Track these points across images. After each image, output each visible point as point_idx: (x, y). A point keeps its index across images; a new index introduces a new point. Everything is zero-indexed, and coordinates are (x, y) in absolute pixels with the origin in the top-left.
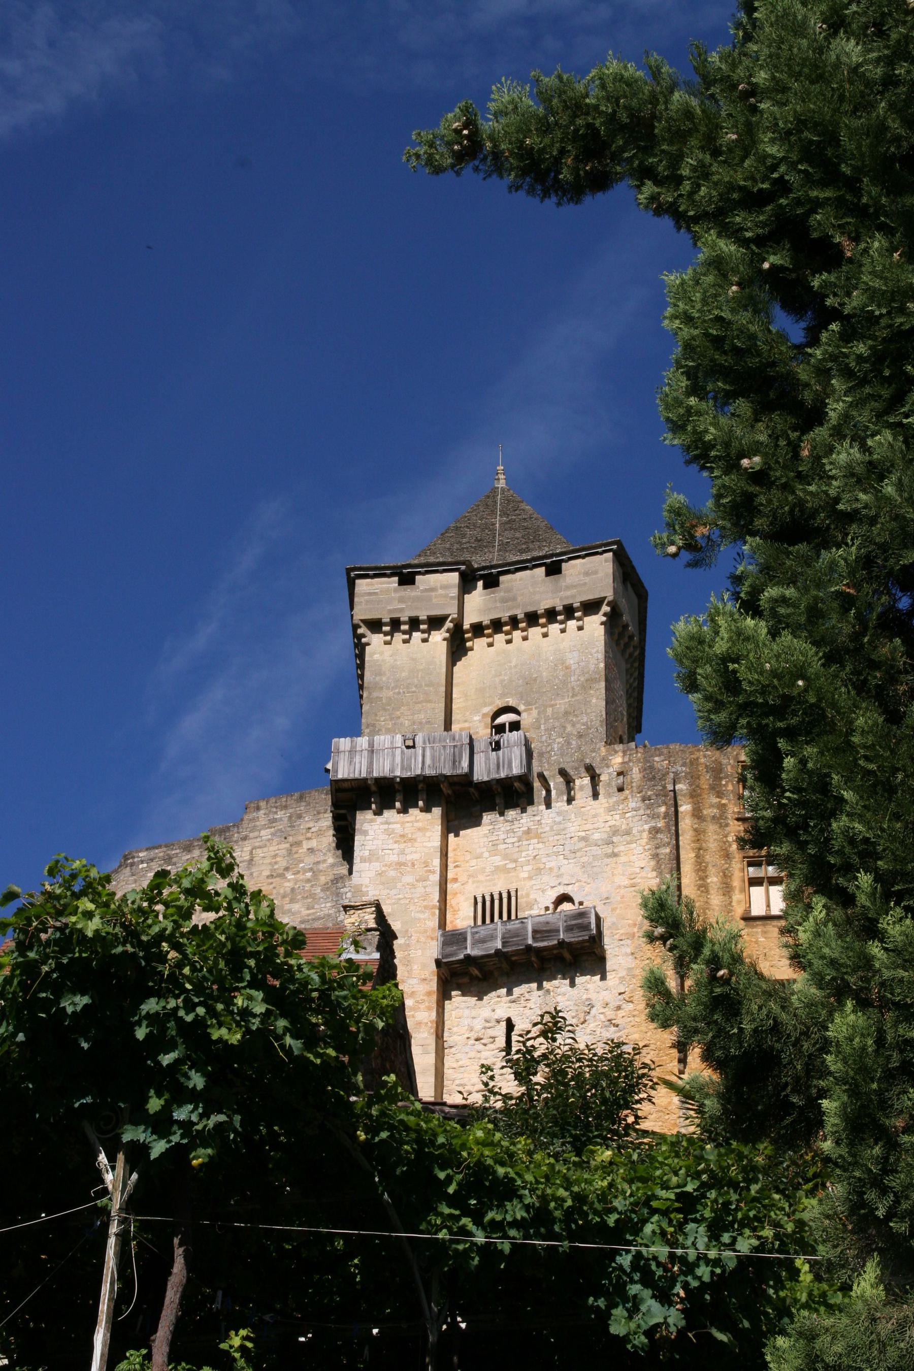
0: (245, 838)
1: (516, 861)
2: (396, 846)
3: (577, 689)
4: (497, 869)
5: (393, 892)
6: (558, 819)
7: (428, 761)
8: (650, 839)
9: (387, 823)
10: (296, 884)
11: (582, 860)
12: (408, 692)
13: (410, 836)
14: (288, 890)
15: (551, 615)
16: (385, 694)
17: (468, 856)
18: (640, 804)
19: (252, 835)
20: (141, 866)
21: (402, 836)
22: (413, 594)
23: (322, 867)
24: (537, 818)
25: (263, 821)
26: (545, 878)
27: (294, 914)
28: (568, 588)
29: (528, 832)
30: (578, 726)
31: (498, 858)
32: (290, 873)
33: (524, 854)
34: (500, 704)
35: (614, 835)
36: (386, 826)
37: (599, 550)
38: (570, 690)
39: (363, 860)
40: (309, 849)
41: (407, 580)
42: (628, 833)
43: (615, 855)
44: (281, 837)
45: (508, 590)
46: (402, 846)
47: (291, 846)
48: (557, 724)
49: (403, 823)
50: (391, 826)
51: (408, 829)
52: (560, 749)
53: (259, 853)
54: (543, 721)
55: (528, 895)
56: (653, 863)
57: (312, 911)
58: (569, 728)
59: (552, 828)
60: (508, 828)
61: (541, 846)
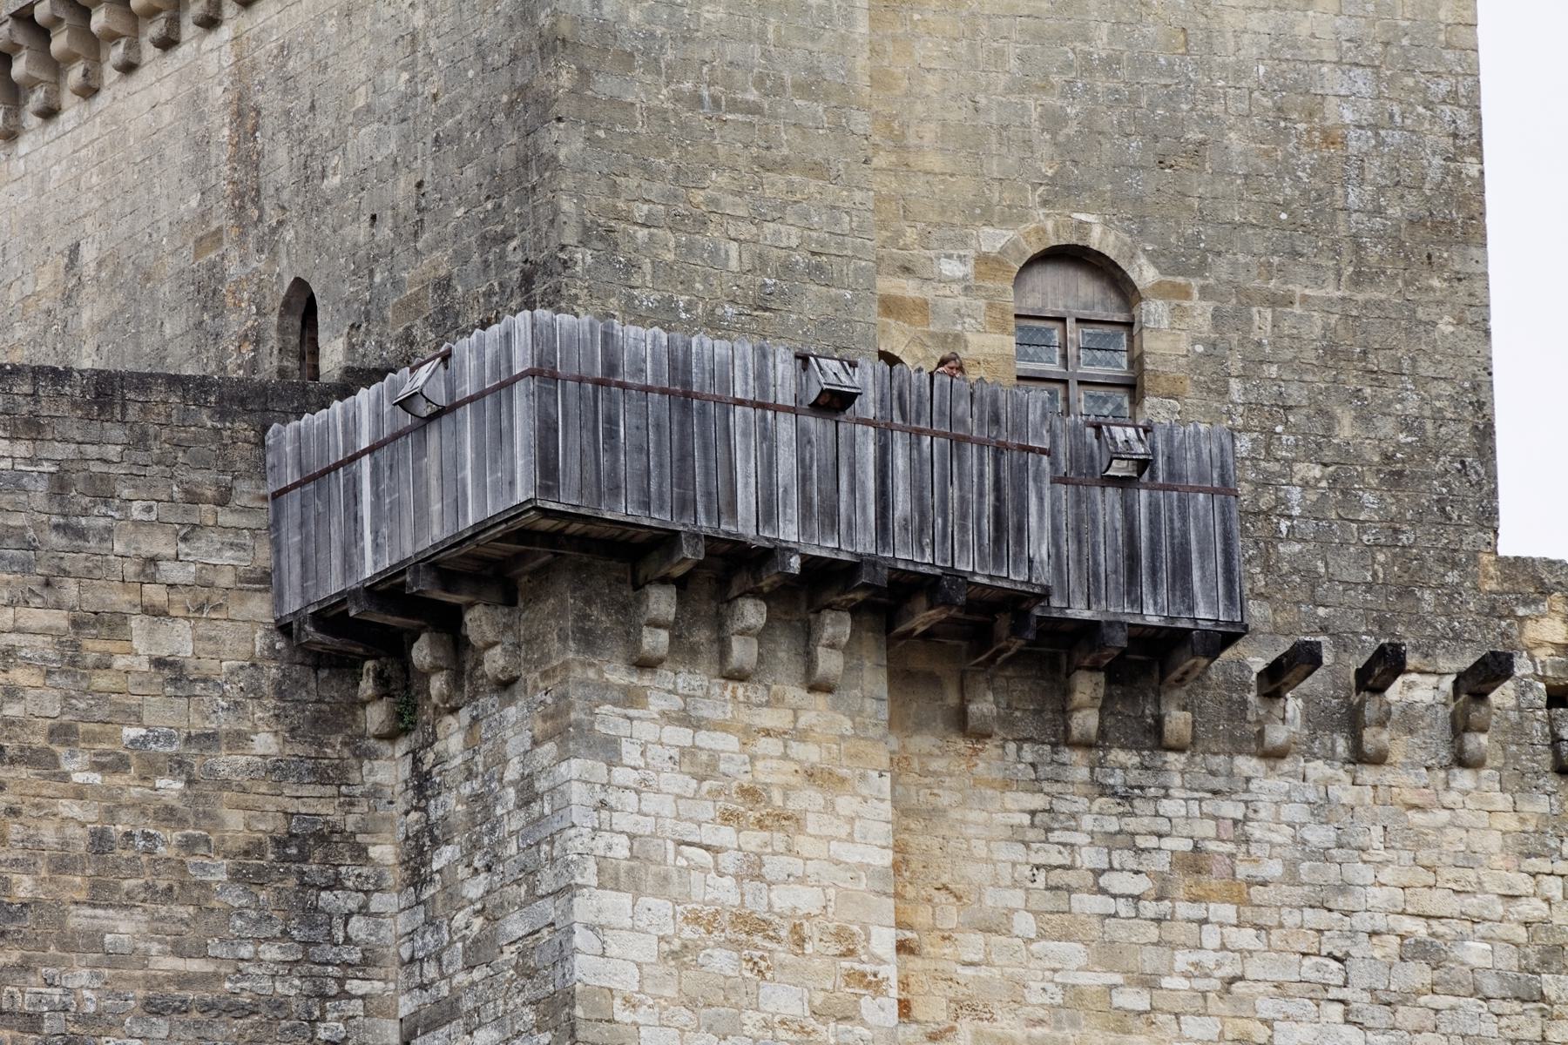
1: (1149, 982)
2: (725, 835)
3: (1374, 252)
6: (1319, 836)
7: (902, 504)
9: (685, 719)
10: (111, 814)
12: (734, 106)
13: (777, 799)
16: (643, 92)
17: (951, 916)
21: (751, 794)
23: (227, 762)
24: (1231, 809)
27: (115, 959)
29: (1195, 861)
30: (1386, 427)
31: (1074, 952)
32: (83, 758)
35: (1545, 963)
36: (683, 736)
38: (1346, 247)
40: (159, 663)
44: (26, 567)
46: (753, 840)
47: (77, 624)
48: (1296, 394)
49: (749, 733)
50: (705, 739)
51: (772, 770)
52: (1314, 512)
54: (1235, 365)
57: (195, 966)
58: (1346, 429)
59: (1292, 867)
60: (1112, 825)
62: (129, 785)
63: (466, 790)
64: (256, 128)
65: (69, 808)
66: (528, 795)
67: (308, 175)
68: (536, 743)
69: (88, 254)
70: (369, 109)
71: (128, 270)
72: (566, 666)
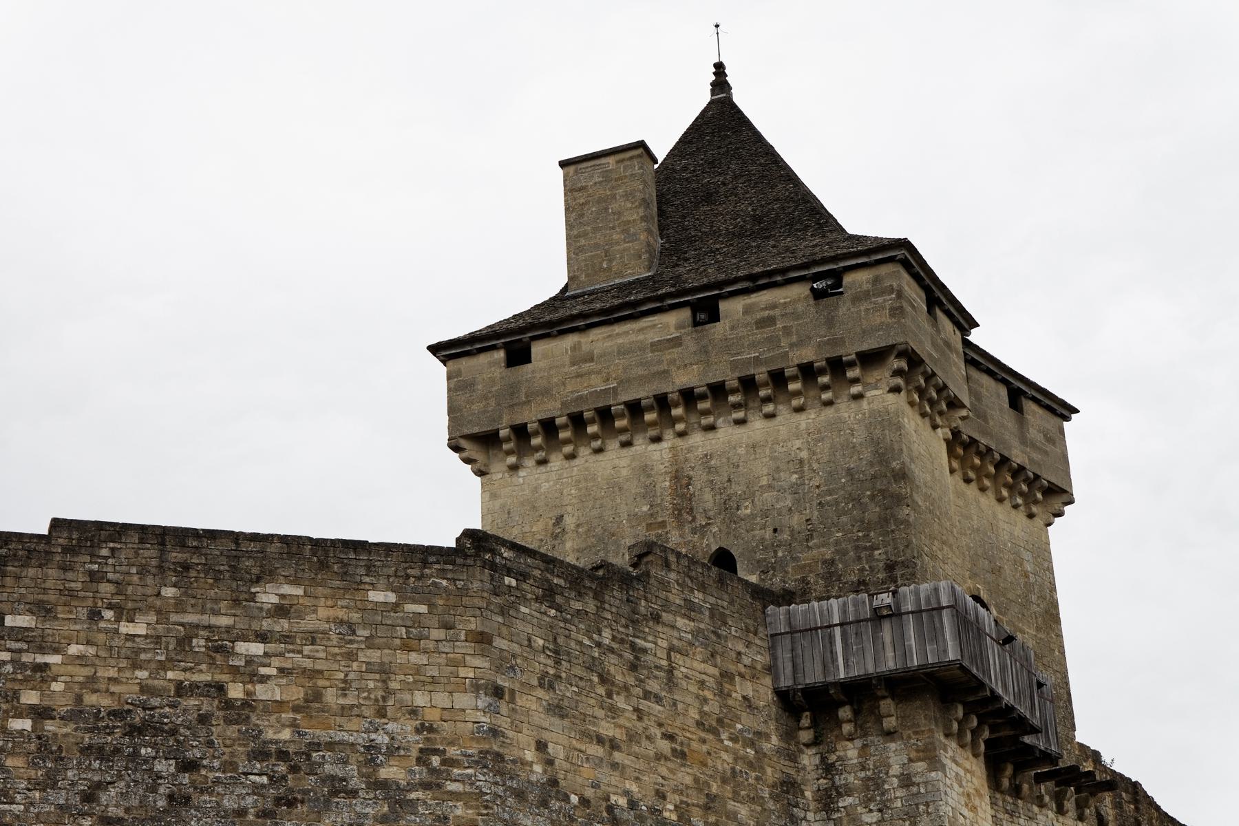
0: (657, 618)
20: (507, 580)
40: (744, 697)
63: (863, 774)
64: (688, 484)
65: (725, 756)
66: (906, 781)
67: (728, 507)
68: (911, 760)
69: (569, 522)
70: (770, 486)
71: (599, 530)
72: (931, 730)
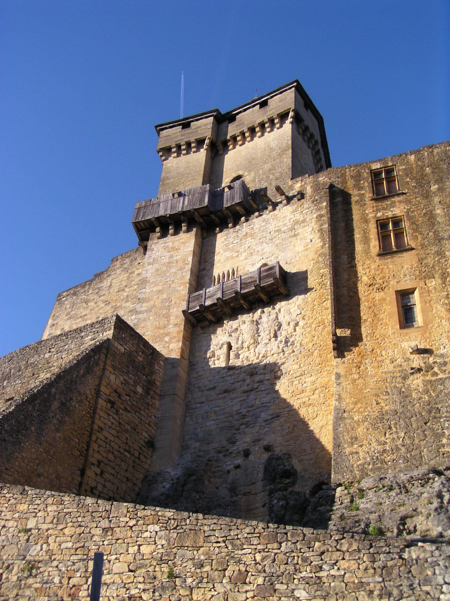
0: (109, 276)
1: (238, 252)
2: (168, 254)
4: (227, 259)
5: (163, 279)
8: (316, 222)
11: (276, 243)
14: (125, 296)
15: (262, 125)
18: (312, 205)
19: (112, 273)
22: (189, 131)
24: (252, 226)
25: (118, 266)
26: (254, 257)
28: (271, 110)
30: (276, 174)
33: (243, 247)
34: (235, 175)
36: (164, 245)
37: (287, 88)
39: (149, 264)
41: (186, 125)
42: (304, 221)
43: (295, 235)
45: (241, 120)
51: (176, 244)
53: (115, 280)
55: (244, 268)
56: (319, 235)
58: (271, 177)
59: (259, 230)
61: (253, 240)
62: (132, 288)
